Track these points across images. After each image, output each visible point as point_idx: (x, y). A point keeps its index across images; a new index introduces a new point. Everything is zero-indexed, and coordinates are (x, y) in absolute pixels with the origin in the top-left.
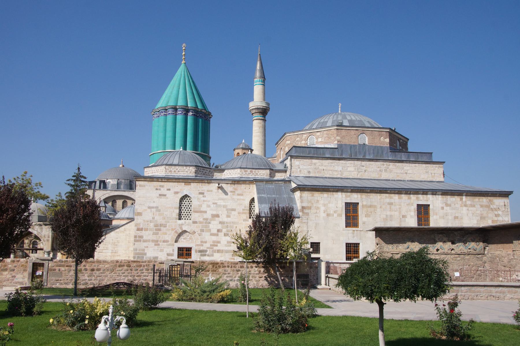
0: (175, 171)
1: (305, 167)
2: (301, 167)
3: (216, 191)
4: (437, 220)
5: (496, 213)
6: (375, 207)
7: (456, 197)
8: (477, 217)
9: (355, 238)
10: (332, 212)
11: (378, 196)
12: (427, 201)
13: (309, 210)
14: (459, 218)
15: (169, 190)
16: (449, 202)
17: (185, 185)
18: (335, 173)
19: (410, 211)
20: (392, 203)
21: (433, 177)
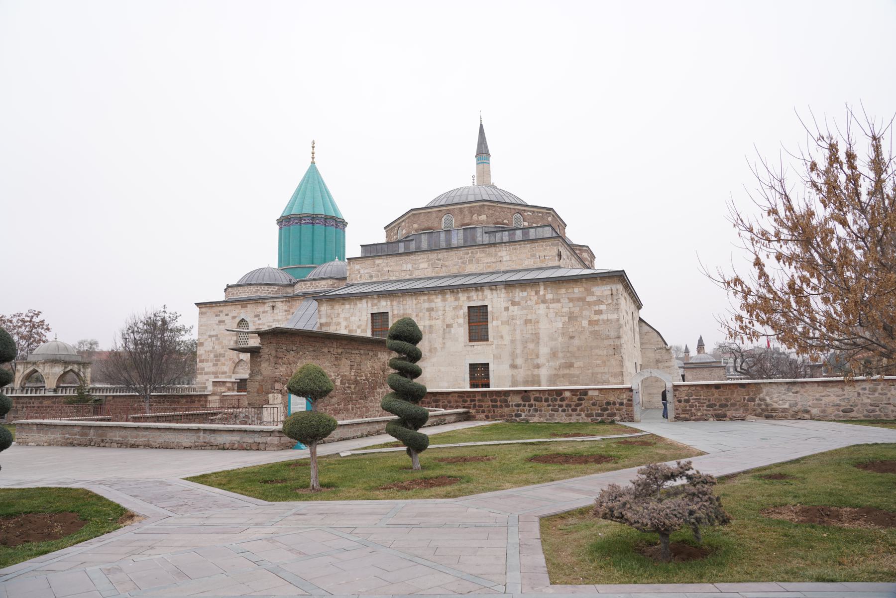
0: (237, 293)
1: (366, 271)
2: (362, 272)
3: (272, 311)
5: (597, 308)
7: (529, 290)
10: (354, 328)
12: (484, 300)
13: (328, 328)
15: (227, 315)
16: (517, 299)
17: (242, 307)
18: (403, 274)
20: (433, 308)
21: (542, 262)
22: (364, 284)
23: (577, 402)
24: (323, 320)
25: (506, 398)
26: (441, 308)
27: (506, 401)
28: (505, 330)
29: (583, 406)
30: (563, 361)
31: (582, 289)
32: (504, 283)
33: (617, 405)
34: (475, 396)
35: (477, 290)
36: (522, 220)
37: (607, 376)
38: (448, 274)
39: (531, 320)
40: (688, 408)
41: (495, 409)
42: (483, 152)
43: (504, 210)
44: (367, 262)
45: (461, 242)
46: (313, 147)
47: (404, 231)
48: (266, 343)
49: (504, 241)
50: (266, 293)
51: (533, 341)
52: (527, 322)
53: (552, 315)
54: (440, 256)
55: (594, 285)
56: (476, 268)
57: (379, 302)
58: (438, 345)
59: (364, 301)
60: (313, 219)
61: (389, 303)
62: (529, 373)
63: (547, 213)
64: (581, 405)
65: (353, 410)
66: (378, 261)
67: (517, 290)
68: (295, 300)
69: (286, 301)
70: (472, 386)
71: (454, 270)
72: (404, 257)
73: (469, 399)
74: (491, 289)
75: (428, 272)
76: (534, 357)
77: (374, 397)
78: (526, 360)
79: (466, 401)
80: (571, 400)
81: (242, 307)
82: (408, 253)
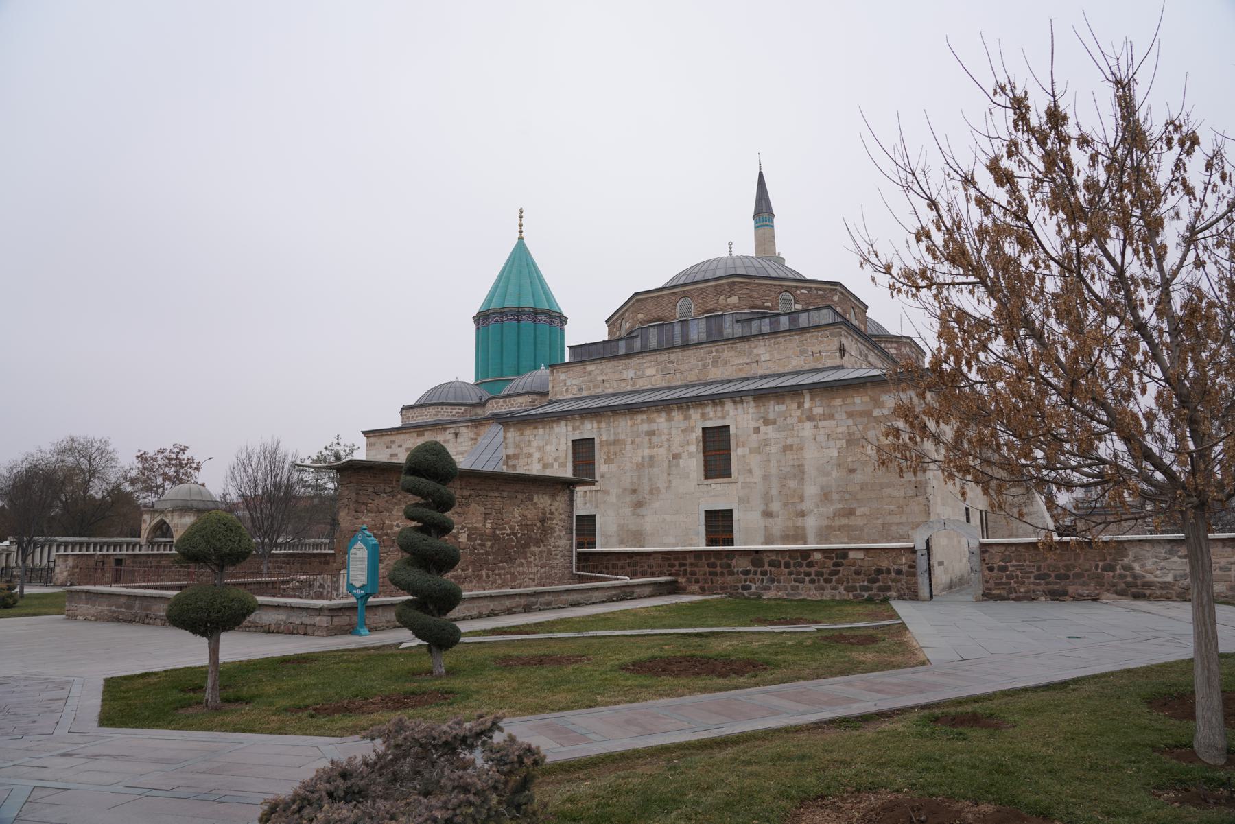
0: (413, 417)
1: (574, 382)
2: (569, 383)
3: (454, 440)
4: (744, 456)
6: (623, 442)
7: (788, 401)
8: (837, 442)
9: (588, 505)
11: (629, 421)
12: (723, 418)
14: (794, 447)
15: (400, 446)
16: (771, 416)
17: (418, 436)
18: (623, 385)
19: (688, 443)
21: (816, 360)
22: (571, 400)
23: (832, 568)
24: (511, 451)
25: (729, 562)
26: (666, 431)
27: (729, 566)
28: (755, 461)
29: (841, 575)
30: (840, 506)
31: (867, 399)
32: (752, 393)
33: (893, 574)
34: (685, 559)
35: (714, 404)
36: (793, 302)
37: (906, 528)
38: (683, 383)
39: (791, 446)
40: (1004, 580)
41: (714, 578)
42: (763, 211)
43: (765, 287)
44: (575, 369)
45: (703, 337)
46: (521, 217)
47: (628, 325)
48: (345, 483)
49: (763, 332)
50: (447, 416)
51: (795, 476)
52: (787, 448)
53: (822, 438)
54: (673, 357)
55: (885, 392)
56: (723, 373)
57: (582, 424)
58: (661, 485)
59: (563, 423)
60: (518, 314)
61: (595, 425)
62: (790, 524)
63: (831, 289)
64: (837, 573)
65: (488, 576)
66: (590, 368)
67: (772, 402)
68: (484, 425)
69: (472, 426)
70: (710, 542)
71: (692, 377)
72: (624, 361)
73: (677, 563)
74: (735, 402)
75: (656, 381)
76: (796, 500)
77: (526, 558)
78: (785, 505)
79: (673, 566)
80: (823, 565)
81: (418, 436)
82: (630, 355)
